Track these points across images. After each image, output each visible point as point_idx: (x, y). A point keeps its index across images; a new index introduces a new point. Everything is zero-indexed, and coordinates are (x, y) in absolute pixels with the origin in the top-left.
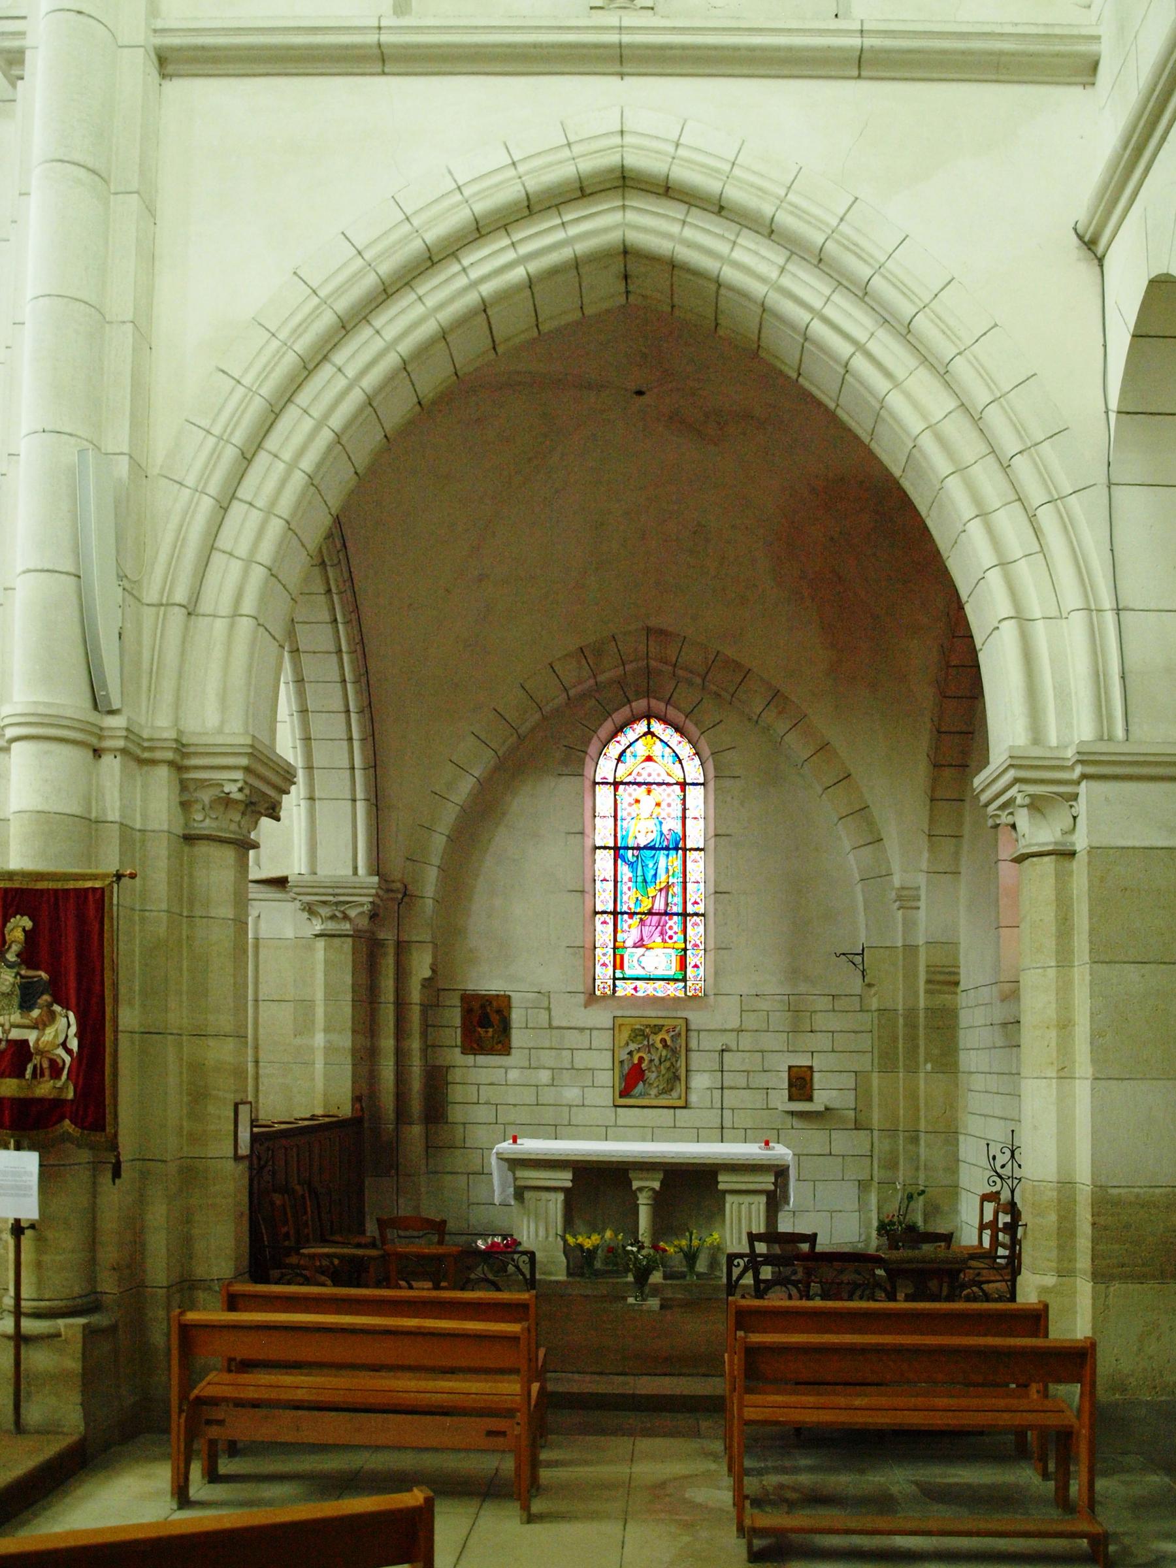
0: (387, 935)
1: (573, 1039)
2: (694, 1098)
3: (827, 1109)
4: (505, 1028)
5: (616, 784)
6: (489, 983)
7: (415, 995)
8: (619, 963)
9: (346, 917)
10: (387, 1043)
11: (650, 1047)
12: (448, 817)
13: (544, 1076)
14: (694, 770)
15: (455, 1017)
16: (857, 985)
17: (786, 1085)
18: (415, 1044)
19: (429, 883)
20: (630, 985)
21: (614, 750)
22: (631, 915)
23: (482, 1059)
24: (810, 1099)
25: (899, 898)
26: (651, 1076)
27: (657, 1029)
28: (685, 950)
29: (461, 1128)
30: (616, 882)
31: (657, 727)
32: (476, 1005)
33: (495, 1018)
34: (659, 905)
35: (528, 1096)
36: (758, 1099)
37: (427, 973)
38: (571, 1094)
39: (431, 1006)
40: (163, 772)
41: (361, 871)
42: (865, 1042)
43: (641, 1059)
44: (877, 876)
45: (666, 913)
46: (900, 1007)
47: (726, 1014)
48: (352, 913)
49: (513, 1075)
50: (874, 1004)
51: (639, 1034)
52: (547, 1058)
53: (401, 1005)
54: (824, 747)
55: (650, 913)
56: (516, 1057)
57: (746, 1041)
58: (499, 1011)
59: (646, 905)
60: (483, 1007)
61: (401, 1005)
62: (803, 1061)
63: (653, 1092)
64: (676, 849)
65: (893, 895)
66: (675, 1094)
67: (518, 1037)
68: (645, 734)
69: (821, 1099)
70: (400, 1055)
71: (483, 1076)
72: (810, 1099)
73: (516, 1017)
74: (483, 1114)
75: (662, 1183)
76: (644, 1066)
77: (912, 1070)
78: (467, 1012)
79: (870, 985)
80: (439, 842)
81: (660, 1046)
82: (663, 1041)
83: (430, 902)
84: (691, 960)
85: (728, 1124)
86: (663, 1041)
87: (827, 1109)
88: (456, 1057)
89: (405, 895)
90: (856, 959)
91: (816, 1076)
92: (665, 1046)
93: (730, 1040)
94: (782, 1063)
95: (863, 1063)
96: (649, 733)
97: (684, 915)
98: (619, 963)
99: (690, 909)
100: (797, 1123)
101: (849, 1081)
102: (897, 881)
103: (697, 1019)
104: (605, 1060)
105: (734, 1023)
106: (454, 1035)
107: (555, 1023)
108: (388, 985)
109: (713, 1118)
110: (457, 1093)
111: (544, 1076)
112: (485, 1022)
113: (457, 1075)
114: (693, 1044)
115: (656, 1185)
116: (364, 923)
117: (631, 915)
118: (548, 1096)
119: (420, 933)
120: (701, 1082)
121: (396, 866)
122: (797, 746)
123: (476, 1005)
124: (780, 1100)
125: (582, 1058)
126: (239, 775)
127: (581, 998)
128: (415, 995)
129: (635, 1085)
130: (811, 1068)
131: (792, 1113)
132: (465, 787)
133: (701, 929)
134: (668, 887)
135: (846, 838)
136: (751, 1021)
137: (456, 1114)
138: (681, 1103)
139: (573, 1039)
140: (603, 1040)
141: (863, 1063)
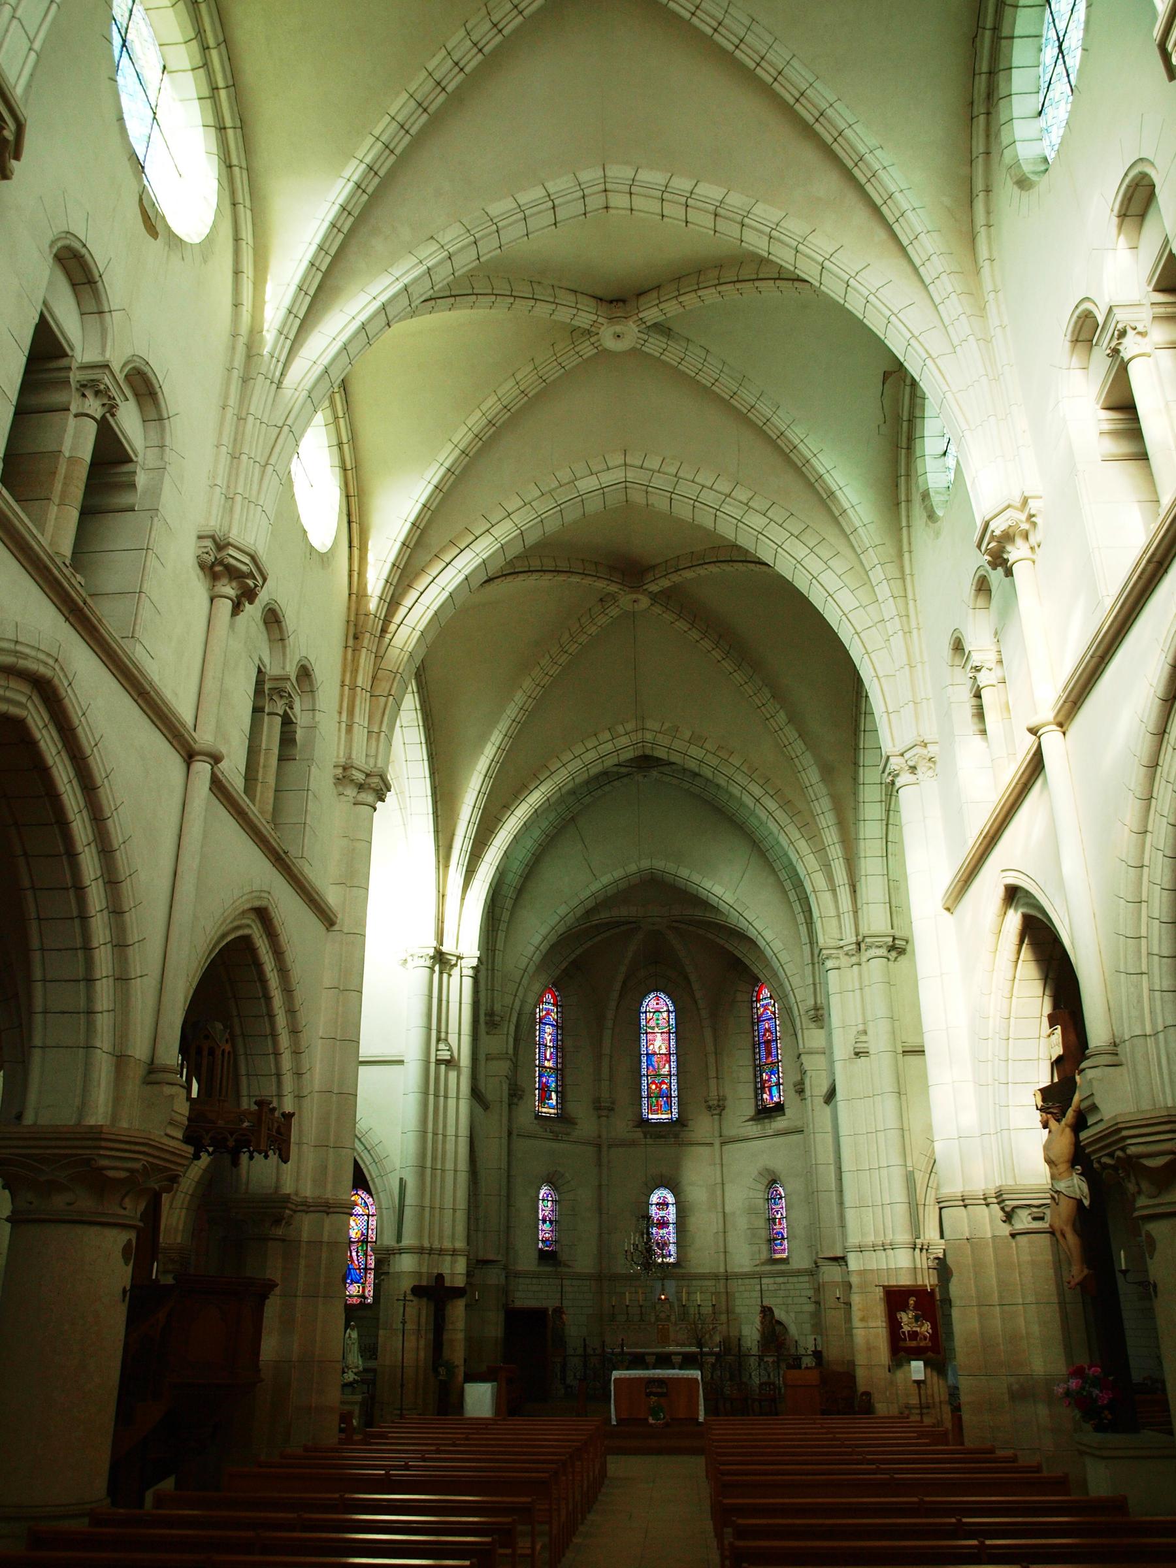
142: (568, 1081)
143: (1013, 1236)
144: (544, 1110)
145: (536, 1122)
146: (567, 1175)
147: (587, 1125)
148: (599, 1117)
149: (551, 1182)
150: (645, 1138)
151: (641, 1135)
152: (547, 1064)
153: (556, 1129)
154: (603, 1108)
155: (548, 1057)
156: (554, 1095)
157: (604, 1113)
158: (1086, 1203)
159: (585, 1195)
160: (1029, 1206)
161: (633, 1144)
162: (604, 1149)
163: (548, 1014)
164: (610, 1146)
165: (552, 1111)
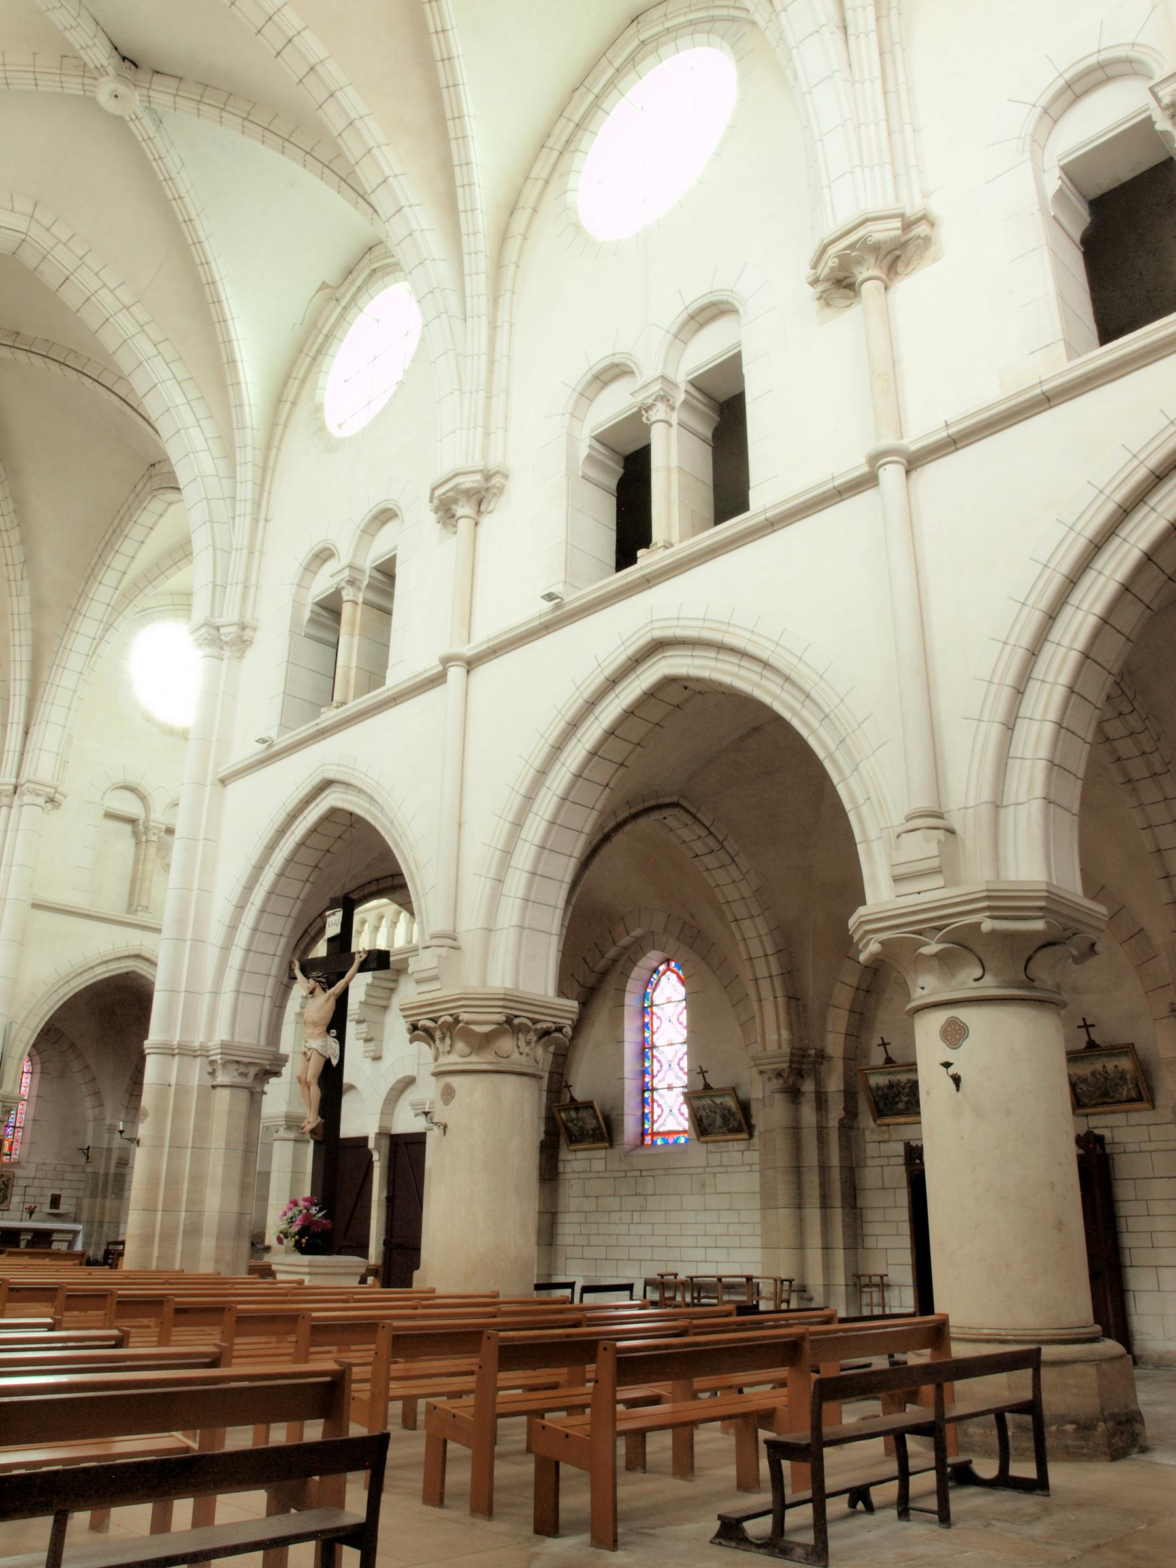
2: (12, 1207)
24: (58, 1208)
42: (82, 1185)
44: (99, 1119)
47: (30, 1171)
50: (89, 1169)
54: (87, 1067)
57: (36, 1183)
62: (57, 1192)
69: (63, 1208)
72: (58, 1208)
75: (33, 1237)
77: (104, 1197)
84: (14, 1147)
90: (86, 1151)
91: (62, 1199)
93: (30, 1182)
94: (49, 1193)
95: (80, 1194)
97: (14, 1127)
101: (74, 1201)
102: (108, 1122)
103: (18, 1172)
105: (32, 1174)
114: (15, 1183)
115: (30, 1238)
122: (76, 1065)
124: (47, 1209)
130: (60, 1195)
133: (20, 1134)
135: (89, 1102)
136: (40, 1174)
143: (214, 1087)
158: (335, 1062)
160: (237, 1062)
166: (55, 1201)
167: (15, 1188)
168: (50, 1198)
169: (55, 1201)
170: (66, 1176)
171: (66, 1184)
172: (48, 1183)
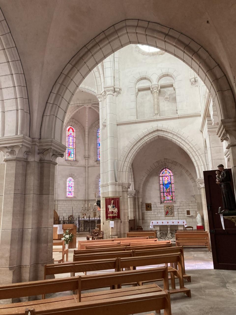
0: (136, 197)
1: (159, 208)
2: (175, 215)
3: (192, 216)
4: (151, 207)
5: (162, 176)
6: (149, 202)
7: (140, 204)
8: (164, 198)
9: (132, 195)
10: (137, 210)
11: (169, 209)
12: (142, 183)
13: (156, 213)
14: (172, 174)
15: (145, 206)
16: (194, 200)
17: (186, 213)
18: (140, 210)
19: (141, 190)
20: (166, 201)
21: (162, 172)
22: (165, 192)
23: (148, 211)
24: (190, 215)
25: (198, 189)
26: (169, 213)
27: (170, 206)
28: (172, 196)
29: (146, 220)
30: (163, 188)
31: (167, 169)
32: (147, 205)
33: (149, 206)
34: (169, 191)
35: (154, 216)
36: (183, 215)
37: (141, 201)
38: (159, 215)
39: (142, 205)
40: (121, 186)
41: (133, 190)
42: (196, 207)
43: (168, 210)
45: (170, 192)
46: (200, 202)
48: (132, 195)
49: (152, 213)
51: (167, 207)
52: (156, 211)
53: (138, 205)
54: (187, 171)
55: (168, 192)
56: (152, 211)
57: (181, 207)
58: (150, 205)
59: (167, 191)
60: (148, 205)
61: (138, 205)
63: (170, 214)
64: (170, 184)
65: (197, 188)
66: (172, 215)
67: (152, 208)
68: (165, 170)
70: (138, 211)
71: (149, 213)
72: (190, 215)
73: (152, 206)
74: (149, 218)
76: (168, 211)
78: (146, 206)
79: (196, 200)
80: (142, 185)
81: (170, 208)
82: (170, 208)
83: (141, 193)
85: (179, 218)
86: (170, 208)
87: (192, 216)
88: (146, 211)
89: (138, 192)
90: (193, 196)
91: (190, 211)
92: (171, 209)
93: (179, 207)
96: (166, 170)
98: (164, 198)
99: (173, 191)
100: (188, 218)
101: (195, 212)
102: (198, 186)
104: (163, 211)
106: (145, 209)
107: (157, 206)
108: (137, 203)
109: (177, 217)
110: (145, 216)
111: (156, 213)
112: (148, 207)
113: (145, 214)
114: (174, 208)
116: (134, 196)
117: (165, 192)
118: (157, 215)
119: (140, 196)
120: (175, 213)
121: (137, 189)
122: (184, 171)
123: (147, 205)
124: (186, 215)
125: (161, 211)
126: (127, 186)
127: (160, 203)
128: (140, 204)
129: (167, 214)
130: (189, 211)
131: (188, 216)
132: (145, 178)
134: (170, 188)
137: (146, 218)
138: (173, 216)
139: (159, 208)
140: (163, 208)
141: (196, 210)
142: (77, 151)
144: (69, 159)
145: (65, 161)
146: (75, 175)
147: (82, 162)
148: (86, 160)
149: (71, 176)
150: (97, 164)
151: (96, 164)
152: (70, 147)
153: (72, 163)
154: (87, 158)
155: (71, 145)
156: (73, 155)
157: (86, 159)
159: (81, 180)
161: (94, 166)
162: (87, 168)
163: (71, 134)
164: (88, 167)
165: (72, 159)
166: (188, 212)
167: (174, 210)
168: (186, 212)
169: (188, 212)
170: (190, 204)
171: (191, 207)
172: (184, 207)
